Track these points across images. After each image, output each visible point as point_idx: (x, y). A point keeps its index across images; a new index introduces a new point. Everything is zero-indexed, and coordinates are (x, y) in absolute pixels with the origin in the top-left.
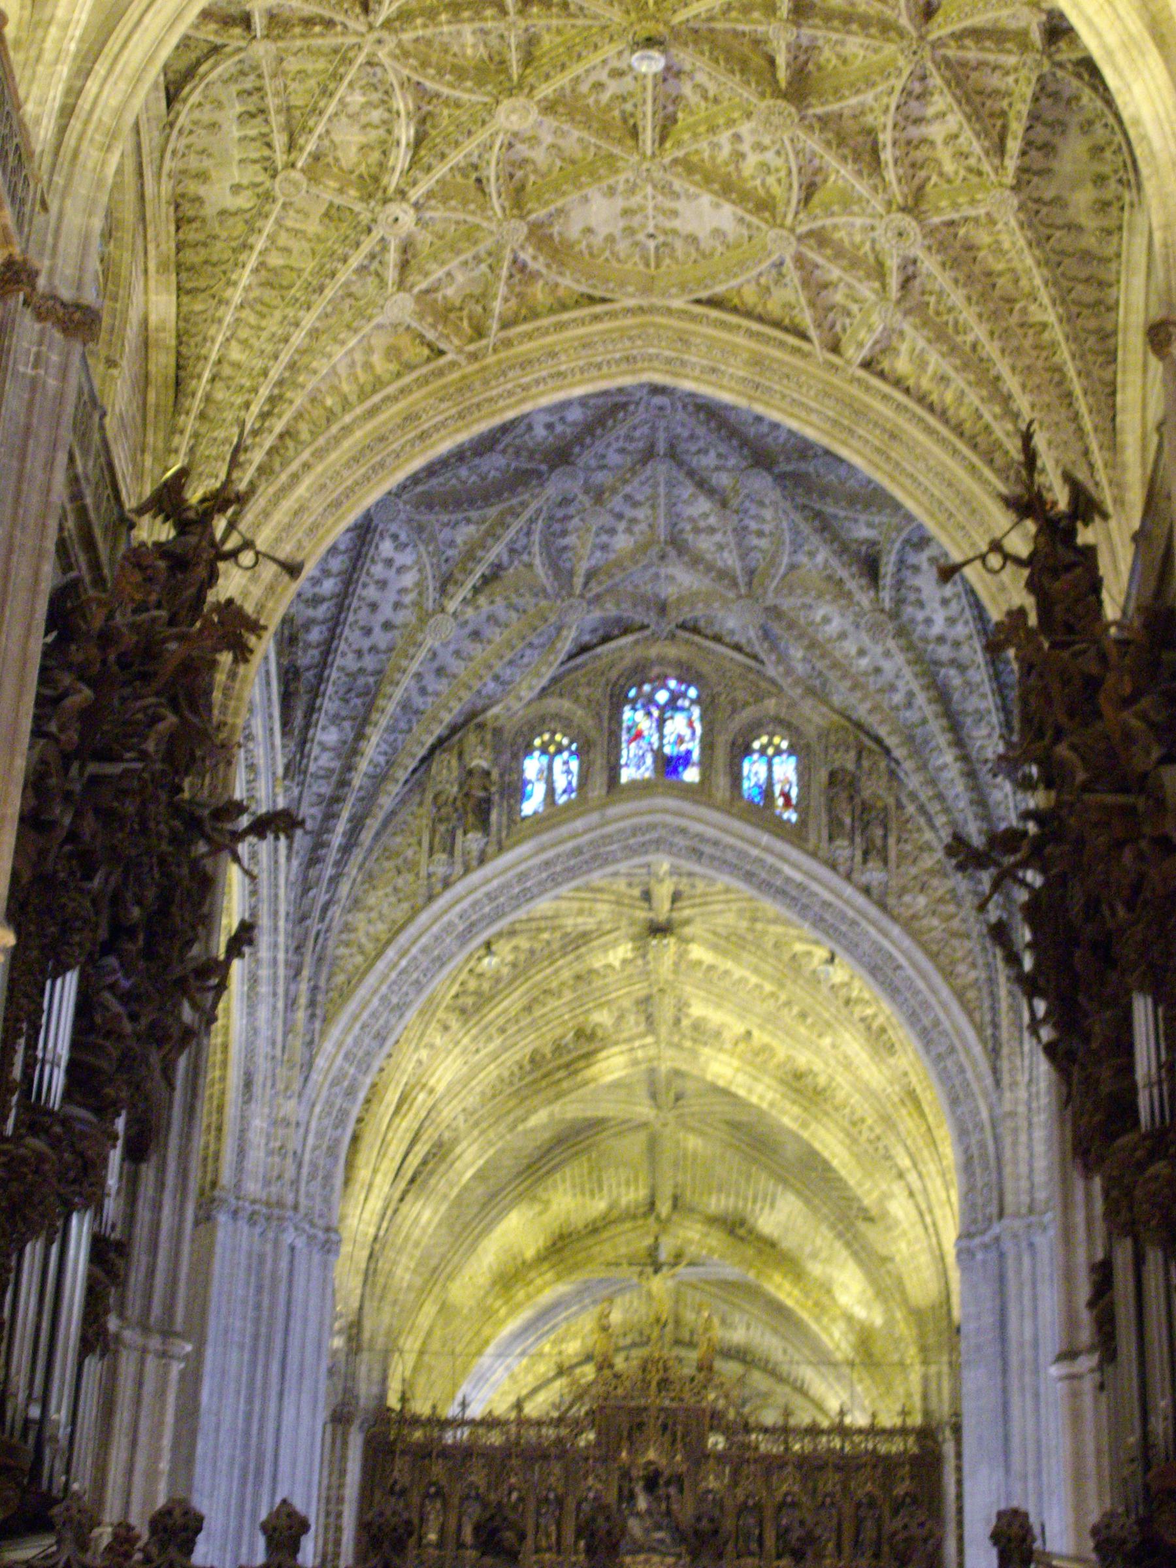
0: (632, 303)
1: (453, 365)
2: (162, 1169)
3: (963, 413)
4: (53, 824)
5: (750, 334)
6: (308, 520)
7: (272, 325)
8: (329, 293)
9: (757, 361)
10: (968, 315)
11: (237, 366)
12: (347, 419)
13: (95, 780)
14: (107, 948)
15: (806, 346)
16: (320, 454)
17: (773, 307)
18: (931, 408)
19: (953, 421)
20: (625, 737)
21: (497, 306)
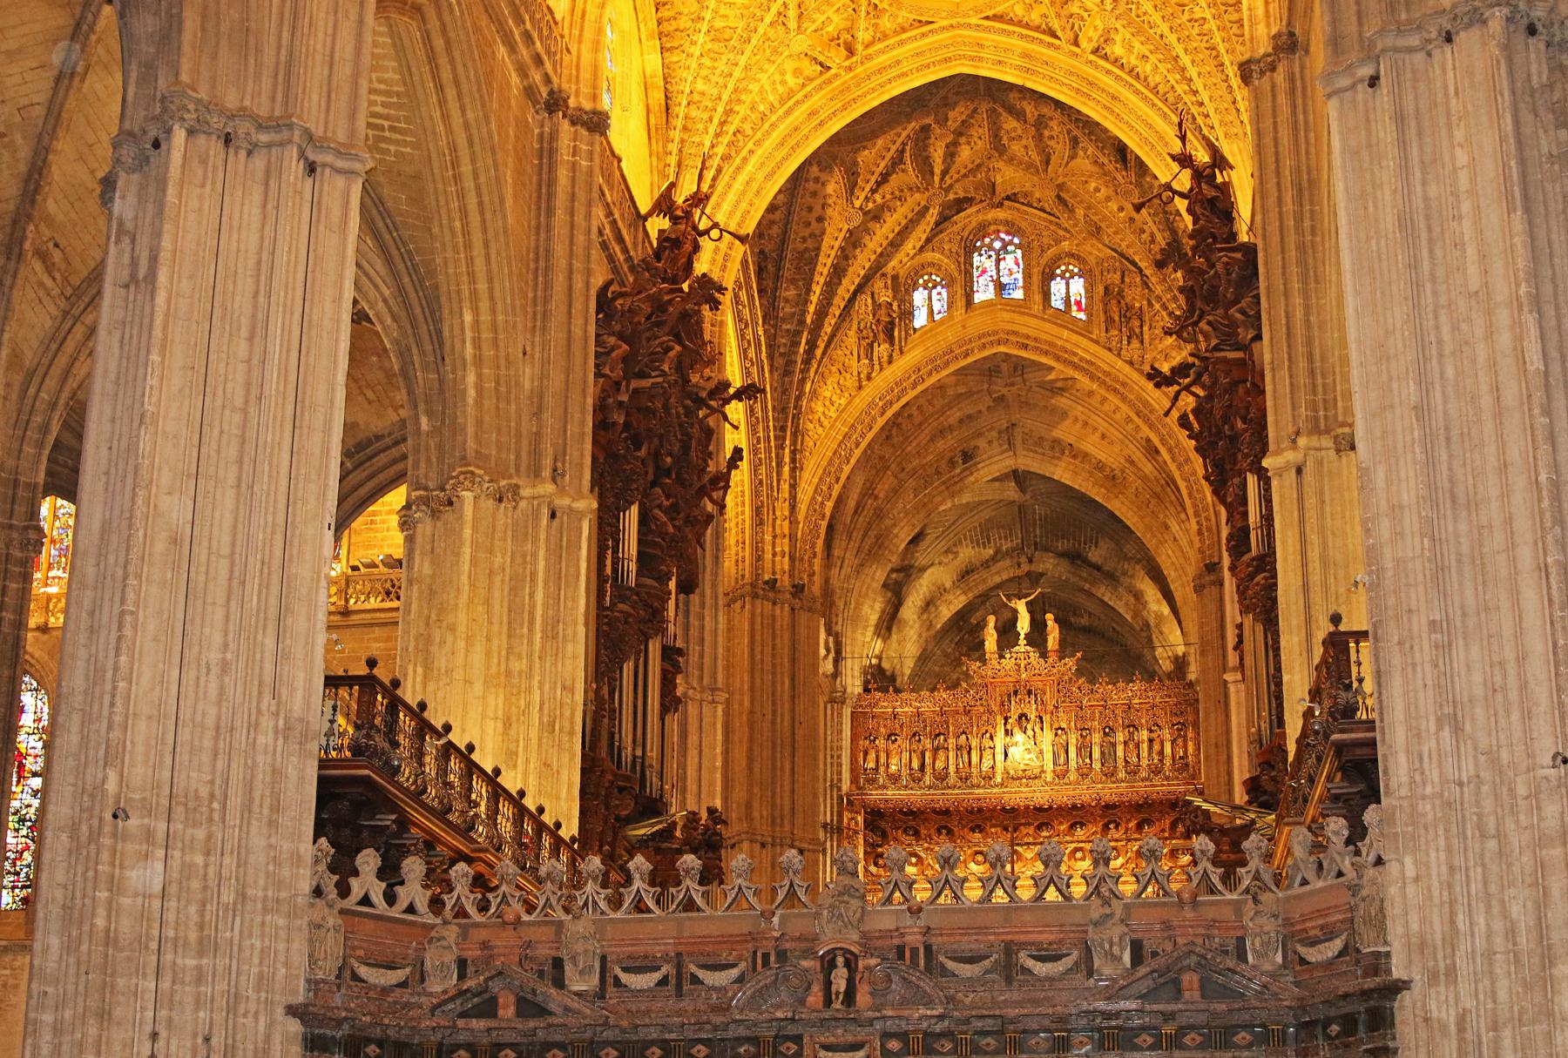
0: (945, 23)
1: (836, 75)
2: (703, 595)
3: (1158, 79)
4: (615, 424)
5: (1022, 36)
6: (755, 186)
7: (721, 66)
8: (754, 41)
9: (1025, 55)
10: (1156, 17)
11: (703, 94)
12: (774, 118)
13: (636, 391)
14: (653, 484)
15: (1057, 42)
16: (758, 143)
17: (1035, 17)
18: (1137, 77)
19: (1152, 85)
20: (976, 274)
21: (863, 35)
